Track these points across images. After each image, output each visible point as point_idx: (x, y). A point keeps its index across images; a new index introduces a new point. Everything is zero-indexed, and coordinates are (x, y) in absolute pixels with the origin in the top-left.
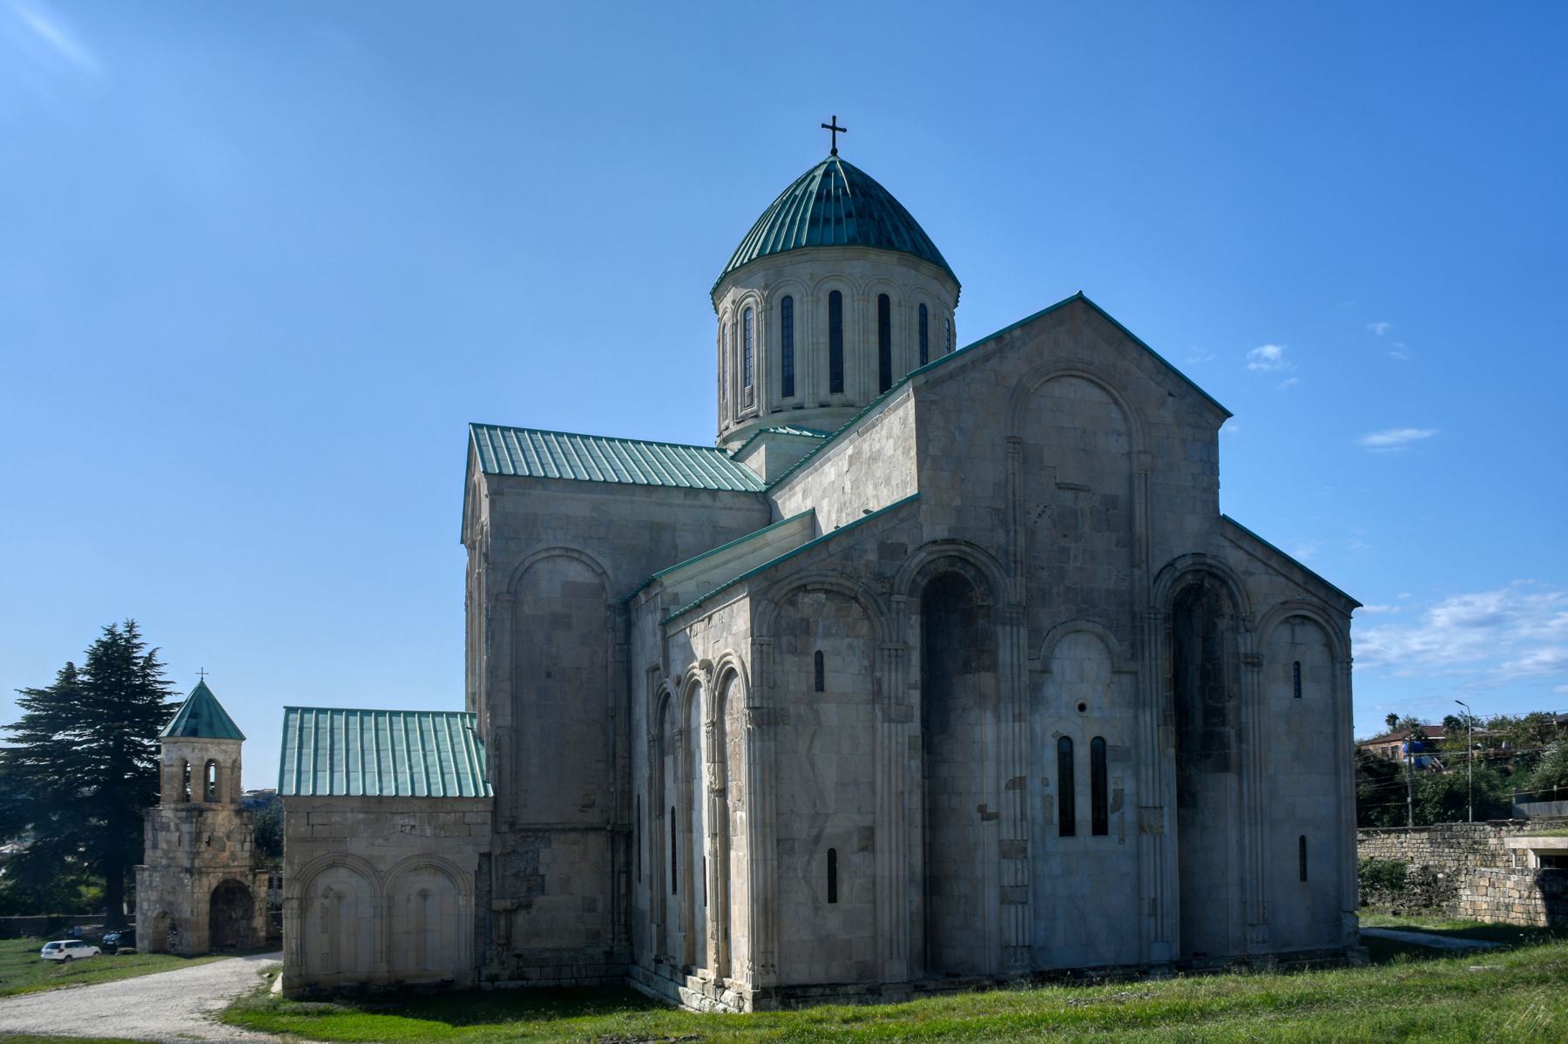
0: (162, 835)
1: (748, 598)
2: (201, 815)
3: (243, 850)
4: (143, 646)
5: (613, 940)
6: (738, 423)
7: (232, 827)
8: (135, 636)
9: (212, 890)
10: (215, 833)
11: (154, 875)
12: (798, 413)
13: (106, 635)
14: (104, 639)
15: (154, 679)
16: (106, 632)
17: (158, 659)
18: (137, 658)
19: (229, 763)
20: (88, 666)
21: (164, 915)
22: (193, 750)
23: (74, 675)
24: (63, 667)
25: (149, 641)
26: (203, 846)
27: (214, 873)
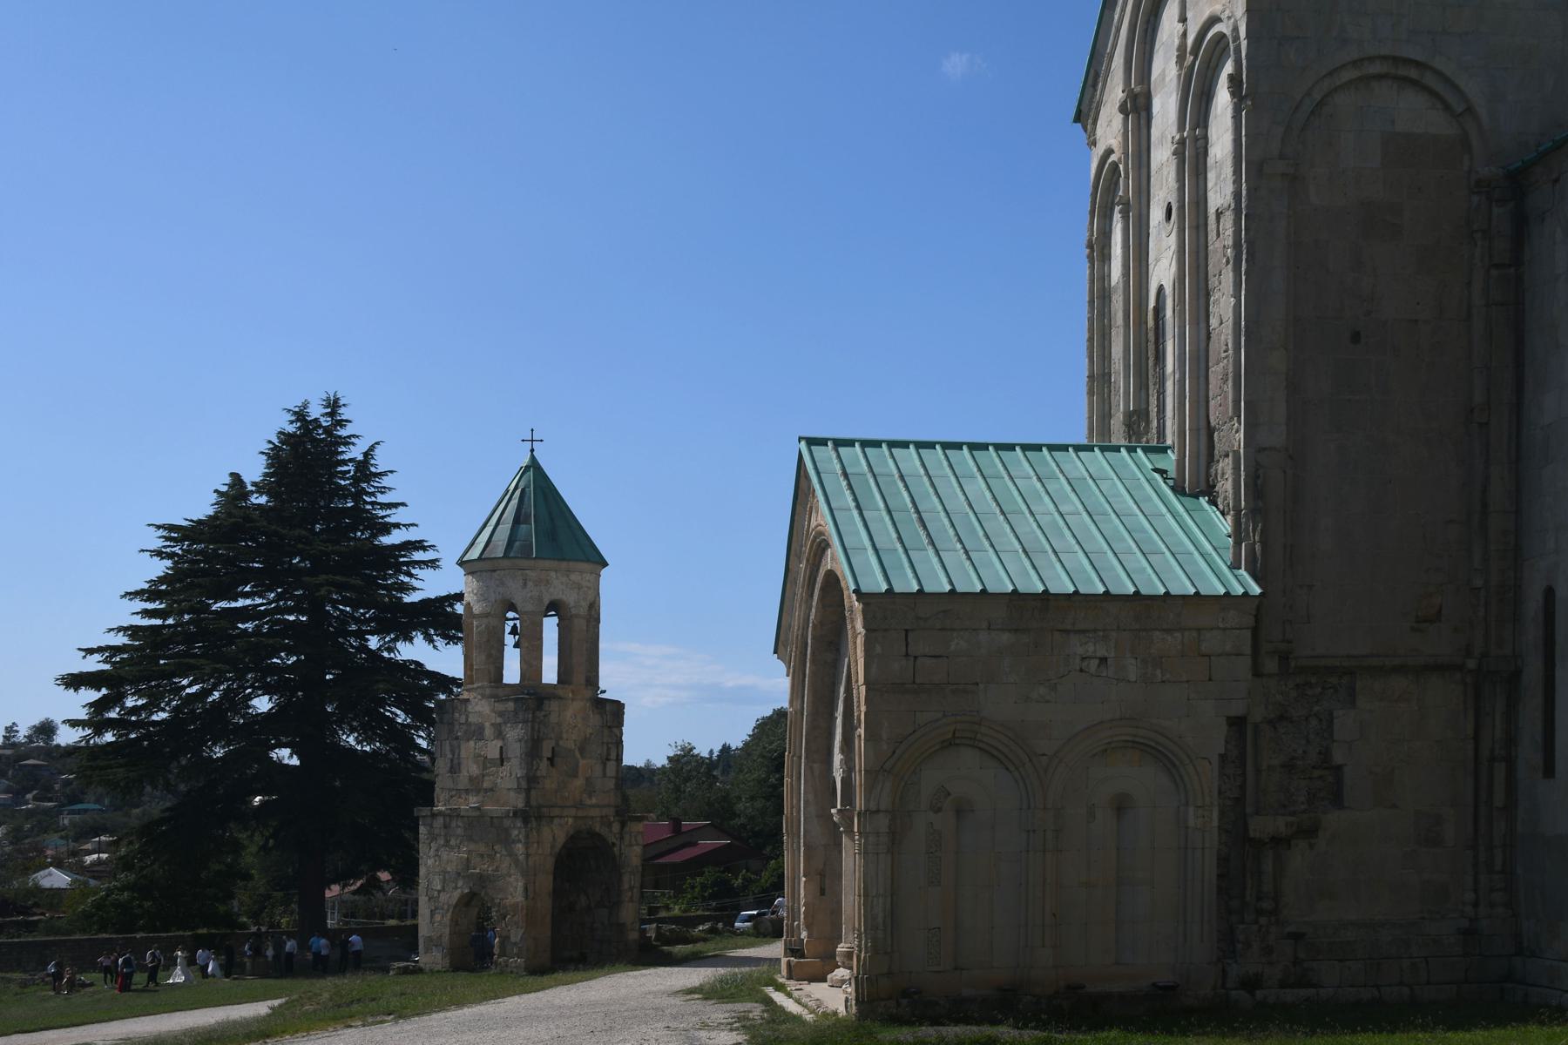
2: (540, 706)
4: (353, 440)
7: (589, 731)
8: (341, 423)
9: (557, 850)
10: (561, 743)
11: (454, 824)
13: (292, 422)
14: (291, 429)
15: (373, 499)
16: (293, 418)
18: (344, 462)
19: (583, 611)
20: (266, 475)
23: (245, 495)
24: (222, 482)
26: (544, 764)
27: (561, 817)
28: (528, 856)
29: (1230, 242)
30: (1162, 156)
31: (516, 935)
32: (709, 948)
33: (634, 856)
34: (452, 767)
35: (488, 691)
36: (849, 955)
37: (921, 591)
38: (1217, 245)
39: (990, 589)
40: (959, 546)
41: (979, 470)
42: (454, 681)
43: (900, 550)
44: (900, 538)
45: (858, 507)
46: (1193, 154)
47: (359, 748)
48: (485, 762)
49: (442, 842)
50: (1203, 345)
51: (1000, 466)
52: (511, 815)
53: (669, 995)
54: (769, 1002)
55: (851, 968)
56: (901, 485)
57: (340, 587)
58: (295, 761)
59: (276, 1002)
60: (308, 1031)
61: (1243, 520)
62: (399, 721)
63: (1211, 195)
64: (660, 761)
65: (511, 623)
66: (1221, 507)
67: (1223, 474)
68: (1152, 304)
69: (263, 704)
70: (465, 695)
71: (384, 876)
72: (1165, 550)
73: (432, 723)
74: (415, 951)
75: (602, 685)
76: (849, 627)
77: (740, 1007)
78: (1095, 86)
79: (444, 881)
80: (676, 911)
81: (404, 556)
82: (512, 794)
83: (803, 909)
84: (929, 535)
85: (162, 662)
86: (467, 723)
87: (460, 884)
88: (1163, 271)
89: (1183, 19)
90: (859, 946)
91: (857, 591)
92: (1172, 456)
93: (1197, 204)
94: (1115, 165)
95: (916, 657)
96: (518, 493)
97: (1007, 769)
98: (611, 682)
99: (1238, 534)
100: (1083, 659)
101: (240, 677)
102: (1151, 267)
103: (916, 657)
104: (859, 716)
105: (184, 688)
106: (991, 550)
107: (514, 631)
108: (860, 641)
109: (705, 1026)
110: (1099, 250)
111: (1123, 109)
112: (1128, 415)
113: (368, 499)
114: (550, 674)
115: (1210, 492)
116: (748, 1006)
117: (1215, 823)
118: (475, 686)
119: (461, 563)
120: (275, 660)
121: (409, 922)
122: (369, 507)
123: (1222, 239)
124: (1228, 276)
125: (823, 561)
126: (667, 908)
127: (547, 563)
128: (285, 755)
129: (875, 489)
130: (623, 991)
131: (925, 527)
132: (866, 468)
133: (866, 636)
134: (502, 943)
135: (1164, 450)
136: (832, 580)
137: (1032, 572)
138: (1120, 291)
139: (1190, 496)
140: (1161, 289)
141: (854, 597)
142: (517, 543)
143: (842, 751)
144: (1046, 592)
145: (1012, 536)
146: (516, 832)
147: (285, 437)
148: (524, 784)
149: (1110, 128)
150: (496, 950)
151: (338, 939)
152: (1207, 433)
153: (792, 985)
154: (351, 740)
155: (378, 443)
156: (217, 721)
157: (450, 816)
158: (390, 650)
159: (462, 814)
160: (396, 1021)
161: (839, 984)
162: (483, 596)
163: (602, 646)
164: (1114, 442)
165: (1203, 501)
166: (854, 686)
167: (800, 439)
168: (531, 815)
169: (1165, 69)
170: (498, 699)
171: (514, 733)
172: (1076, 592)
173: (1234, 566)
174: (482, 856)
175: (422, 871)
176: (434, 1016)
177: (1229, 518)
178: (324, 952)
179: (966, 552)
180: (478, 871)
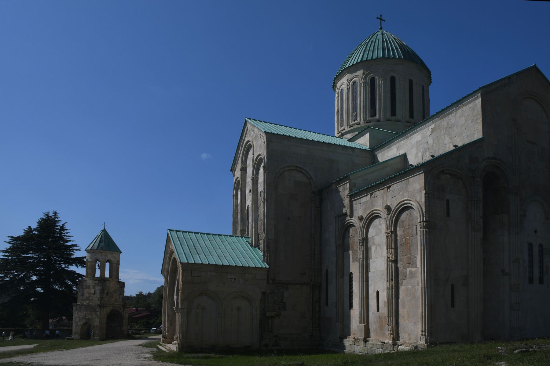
0: (86, 291)
1: (424, 174)
3: (120, 298)
4: (60, 221)
5: (313, 330)
8: (57, 218)
12: (378, 123)
13: (45, 216)
14: (44, 217)
16: (45, 215)
17: (66, 227)
18: (57, 226)
19: (116, 262)
20: (37, 227)
21: (85, 324)
22: (101, 256)
23: (32, 231)
24: (26, 228)
25: (62, 219)
26: (105, 295)
28: (100, 315)
29: (263, 198)
30: (249, 180)
31: (97, 332)
32: (144, 336)
33: (127, 316)
35: (91, 278)
36: (177, 338)
37: (195, 263)
38: (260, 198)
39: (210, 263)
40: (204, 254)
41: (208, 239)
42: (83, 275)
43: (190, 254)
44: (190, 252)
45: (181, 245)
46: (255, 180)
47: (58, 289)
48: (90, 294)
49: (79, 311)
50: (257, 218)
51: (213, 238)
52: (97, 305)
53: (134, 346)
54: (158, 348)
55: (177, 341)
56: (191, 241)
57: (55, 253)
58: (42, 291)
59: (36, 345)
60: (44, 352)
61: (265, 253)
62: (69, 283)
63: (259, 188)
64: (134, 295)
65: (98, 264)
66: (261, 250)
67: (261, 243)
68: (246, 209)
69: (34, 278)
70: (86, 279)
71: (64, 318)
72: (249, 258)
73: (77, 284)
74: (72, 334)
75: (120, 278)
76: (178, 269)
77: (151, 349)
78: (235, 165)
80: (136, 328)
81: (71, 248)
82: (97, 301)
83: (166, 328)
84: (197, 251)
85: (8, 267)
87: (83, 320)
88: (249, 202)
89: (253, 154)
90: (179, 336)
91: (180, 262)
92: (250, 239)
93: (256, 190)
94: (239, 181)
95: (193, 276)
96: (101, 236)
97: (214, 300)
98: (122, 277)
99: (264, 255)
101: (29, 271)
102: (246, 202)
103: (193, 276)
104: (180, 288)
105: (15, 273)
106: (211, 255)
107: (98, 266)
108: (181, 272)
109: (143, 353)
110: (235, 197)
111: (241, 170)
112: (241, 230)
113: (63, 234)
114: (107, 275)
115: (258, 247)
116: (153, 349)
117: (259, 313)
118: (88, 277)
119: (86, 250)
120: (38, 268)
121: (70, 328)
122: (63, 236)
123: (261, 197)
124: (262, 205)
125: (173, 255)
126: (134, 327)
127: (107, 252)
128: (39, 289)
129: (185, 241)
130: (123, 345)
131: (196, 250)
132: (183, 237)
133: (182, 271)
134: (93, 334)
135: (249, 238)
136: (175, 259)
137: (220, 260)
138: (240, 205)
139: (254, 247)
140: (248, 206)
141: (180, 263)
142: (100, 247)
143: (176, 295)
144: (223, 265)
145: (215, 253)
146: (97, 309)
147: (43, 220)
148: (100, 299)
149: (238, 173)
150: (92, 335)
151: (52, 332)
152: (258, 235)
153: (164, 344)
154: (57, 287)
155: (66, 223)
156: (22, 281)
157: (81, 305)
158: (67, 267)
160: (66, 350)
161: (175, 344)
162: (91, 258)
163: (120, 269)
164: (238, 235)
165: (257, 248)
166: (179, 282)
167: (168, 230)
168: (101, 306)
169: (250, 163)
170: (94, 280)
171: (98, 288)
172: (229, 265)
173: (263, 262)
174: (89, 314)
175: (74, 317)
176: (76, 349)
177: (262, 252)
178: (49, 334)
179: (205, 255)
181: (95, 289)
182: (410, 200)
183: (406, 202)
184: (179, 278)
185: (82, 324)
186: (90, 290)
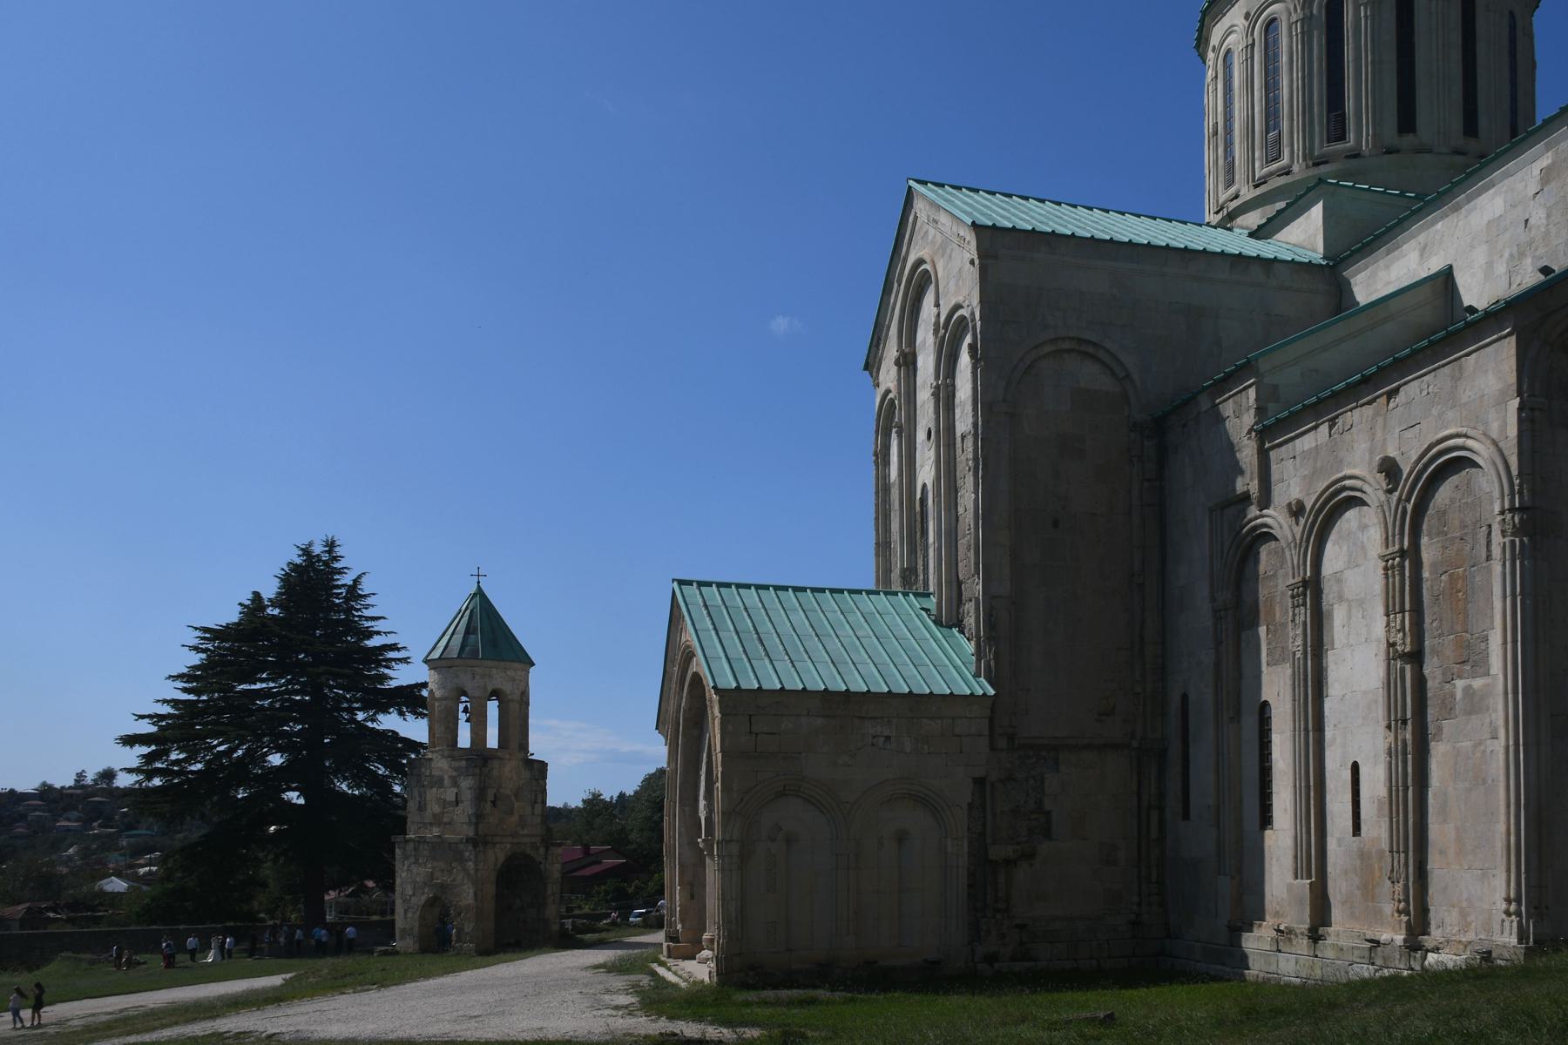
2: (485, 765)
3: (533, 814)
4: (345, 570)
6: (1256, 186)
8: (336, 559)
10: (501, 790)
11: (421, 848)
13: (300, 556)
14: (298, 561)
16: (301, 553)
17: (366, 587)
19: (517, 697)
20: (279, 593)
23: (264, 608)
24: (246, 598)
25: (353, 563)
26: (488, 806)
27: (501, 843)
28: (477, 870)
29: (971, 456)
30: (924, 396)
31: (468, 927)
32: (611, 936)
33: (555, 870)
34: (419, 807)
35: (446, 753)
36: (711, 941)
37: (760, 688)
38: (963, 458)
40: (787, 658)
41: (800, 605)
42: (421, 745)
43: (745, 660)
44: (745, 651)
45: (715, 629)
46: (945, 396)
47: (350, 792)
48: (444, 804)
49: (412, 860)
50: (953, 525)
51: (815, 603)
52: (464, 841)
53: (582, 970)
54: (654, 974)
55: (713, 950)
56: (745, 614)
57: (335, 676)
58: (302, 801)
59: (288, 976)
60: (312, 996)
61: (982, 644)
62: (380, 772)
63: (957, 424)
64: (576, 802)
65: (464, 705)
66: (967, 635)
67: (968, 613)
68: (918, 496)
69: (276, 760)
70: (430, 755)
71: (370, 884)
72: (930, 664)
73: (405, 774)
74: (392, 937)
75: (531, 750)
76: (709, 712)
77: (633, 978)
78: (878, 345)
79: (414, 888)
80: (586, 909)
81: (382, 655)
82: (465, 826)
83: (678, 909)
84: (765, 649)
85: (198, 727)
86: (431, 775)
87: (426, 890)
88: (926, 474)
89: (937, 305)
90: (719, 935)
91: (715, 687)
92: (934, 599)
93: (949, 429)
94: (892, 401)
96: (468, 611)
97: (822, 812)
98: (538, 747)
99: (979, 653)
100: (874, 737)
101: (259, 738)
102: (917, 471)
103: (757, 734)
104: (717, 774)
105: (216, 746)
106: (809, 661)
107: (466, 710)
108: (717, 722)
109: (608, 991)
110: (882, 457)
111: (897, 363)
112: (903, 571)
113: (356, 614)
114: (492, 741)
115: (959, 624)
116: (640, 977)
117: (966, 849)
118: (437, 749)
119: (426, 661)
120: (285, 728)
121: (389, 918)
122: (356, 619)
123: (966, 454)
124: (970, 479)
125: (691, 666)
126: (580, 908)
127: (490, 663)
128: (294, 797)
129: (727, 617)
130: (548, 967)
131: (763, 645)
132: (720, 602)
133: (721, 718)
134: (458, 933)
135: (928, 595)
136: (697, 680)
137: (838, 677)
138: (897, 487)
139: (945, 627)
140: (924, 486)
141: (713, 692)
142: (467, 648)
143: (705, 798)
144: (847, 690)
145: (823, 651)
146: (467, 854)
147: (295, 567)
148: (474, 820)
149: (889, 376)
150: (454, 938)
151: (336, 930)
152: (957, 584)
153: (671, 962)
154: (344, 787)
155: (364, 574)
156: (240, 772)
157: (418, 842)
158: (373, 721)
159: (428, 840)
160: (379, 989)
161: (704, 961)
162: (442, 686)
163: (530, 721)
164: (894, 589)
165: (955, 630)
166: (714, 754)
167: (673, 580)
168: (479, 842)
169: (926, 338)
170: (453, 758)
171: (466, 783)
172: (869, 691)
173: (977, 675)
174: (443, 871)
175: (398, 881)
176: (408, 985)
178: (324, 939)
179: (792, 662)
180: (439, 881)
181: (458, 787)
182: (1466, 436)
183: (1451, 442)
184: (712, 743)
185: (423, 902)
186: (442, 790)
